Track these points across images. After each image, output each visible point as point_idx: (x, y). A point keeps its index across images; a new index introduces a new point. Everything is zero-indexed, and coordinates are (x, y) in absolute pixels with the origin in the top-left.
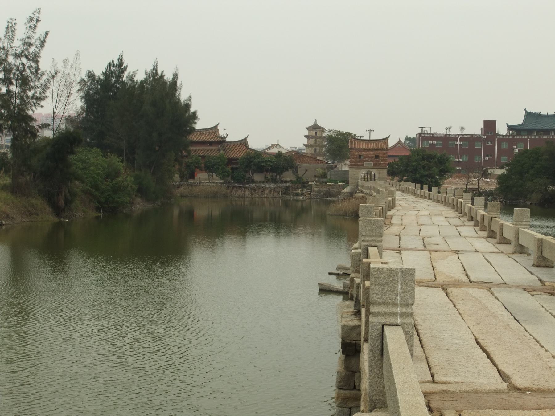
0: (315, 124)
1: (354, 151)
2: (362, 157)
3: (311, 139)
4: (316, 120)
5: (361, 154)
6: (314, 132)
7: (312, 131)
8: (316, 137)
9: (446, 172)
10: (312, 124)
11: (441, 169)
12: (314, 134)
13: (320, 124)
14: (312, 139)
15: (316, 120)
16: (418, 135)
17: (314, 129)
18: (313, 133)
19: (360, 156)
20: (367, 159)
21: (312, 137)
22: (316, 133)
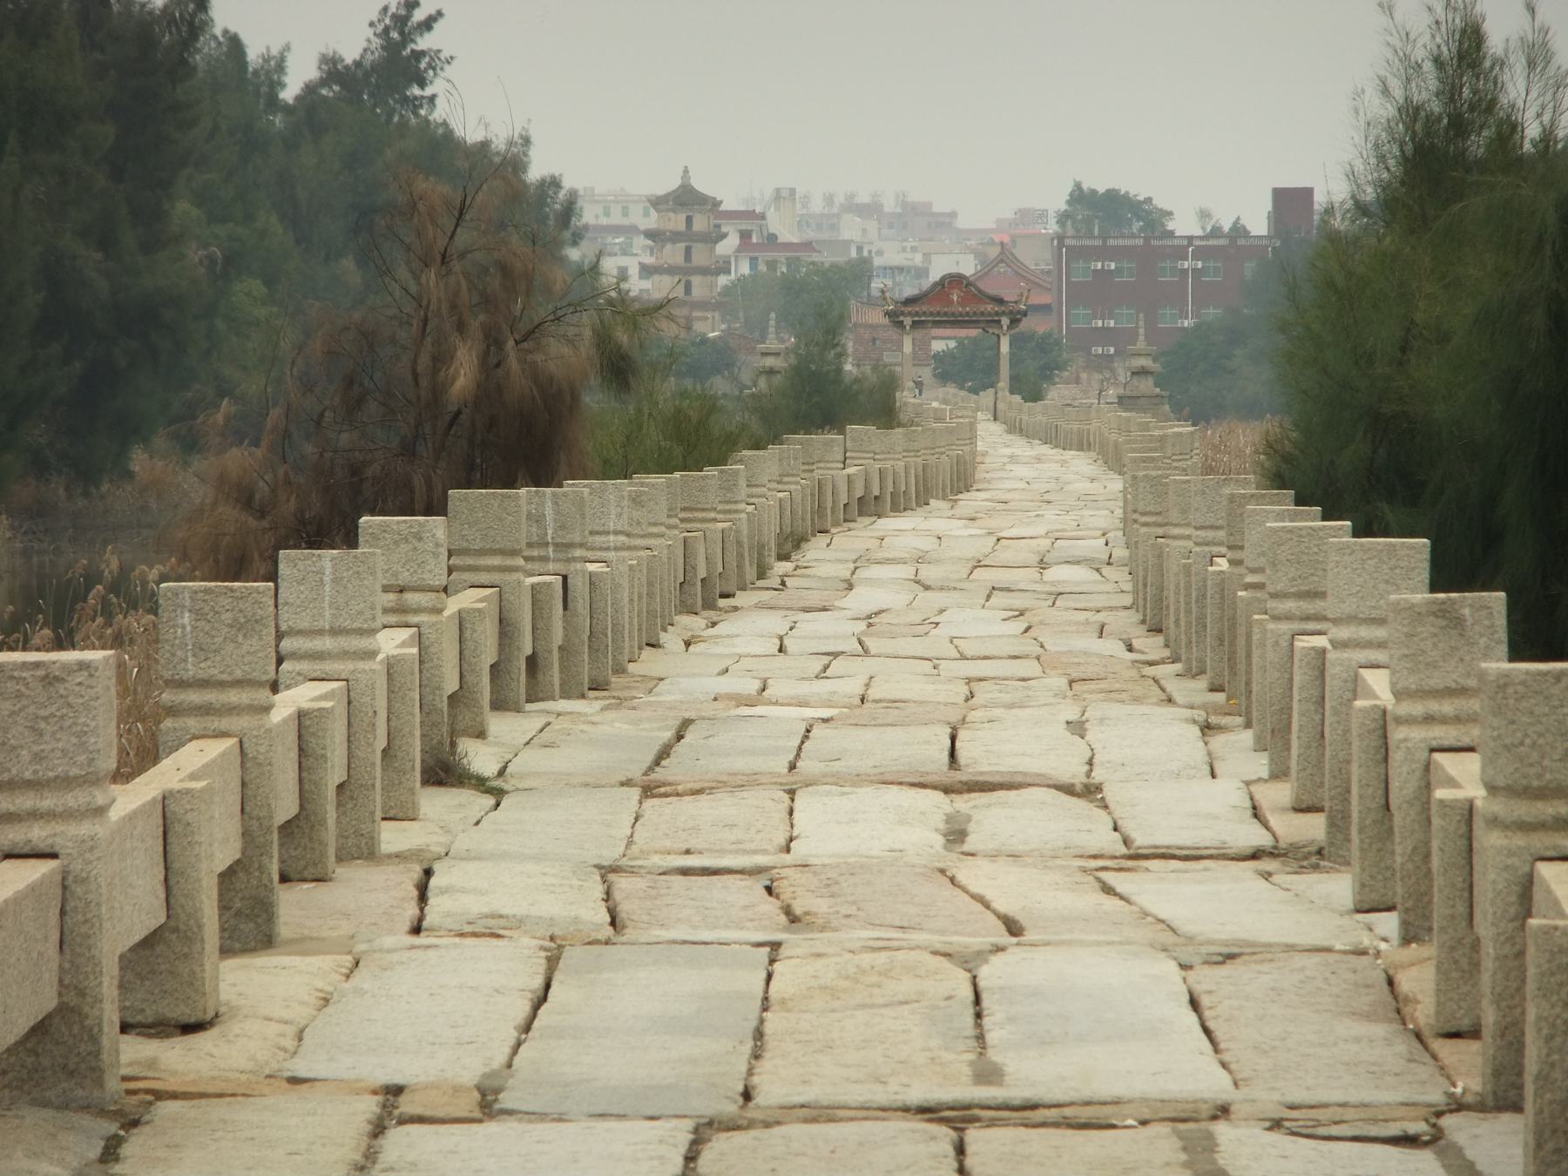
0: (680, 187)
1: (862, 331)
2: (877, 342)
3: (669, 246)
4: (686, 171)
5: (876, 336)
6: (682, 217)
7: (671, 215)
8: (687, 236)
9: (1053, 369)
10: (670, 183)
11: (1042, 362)
12: (682, 227)
13: (701, 185)
14: (674, 242)
15: (686, 171)
16: (1055, 242)
17: (680, 205)
18: (677, 222)
19: (874, 340)
20: (889, 346)
21: (675, 237)
22: (689, 220)
